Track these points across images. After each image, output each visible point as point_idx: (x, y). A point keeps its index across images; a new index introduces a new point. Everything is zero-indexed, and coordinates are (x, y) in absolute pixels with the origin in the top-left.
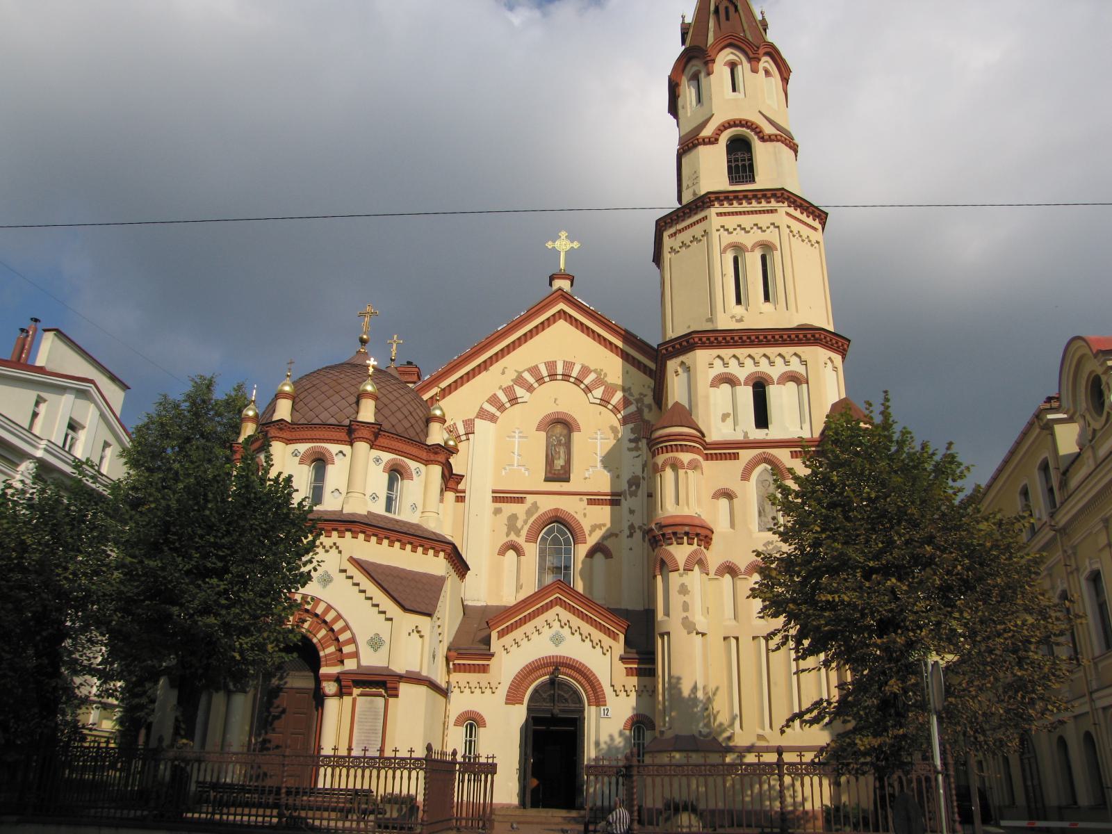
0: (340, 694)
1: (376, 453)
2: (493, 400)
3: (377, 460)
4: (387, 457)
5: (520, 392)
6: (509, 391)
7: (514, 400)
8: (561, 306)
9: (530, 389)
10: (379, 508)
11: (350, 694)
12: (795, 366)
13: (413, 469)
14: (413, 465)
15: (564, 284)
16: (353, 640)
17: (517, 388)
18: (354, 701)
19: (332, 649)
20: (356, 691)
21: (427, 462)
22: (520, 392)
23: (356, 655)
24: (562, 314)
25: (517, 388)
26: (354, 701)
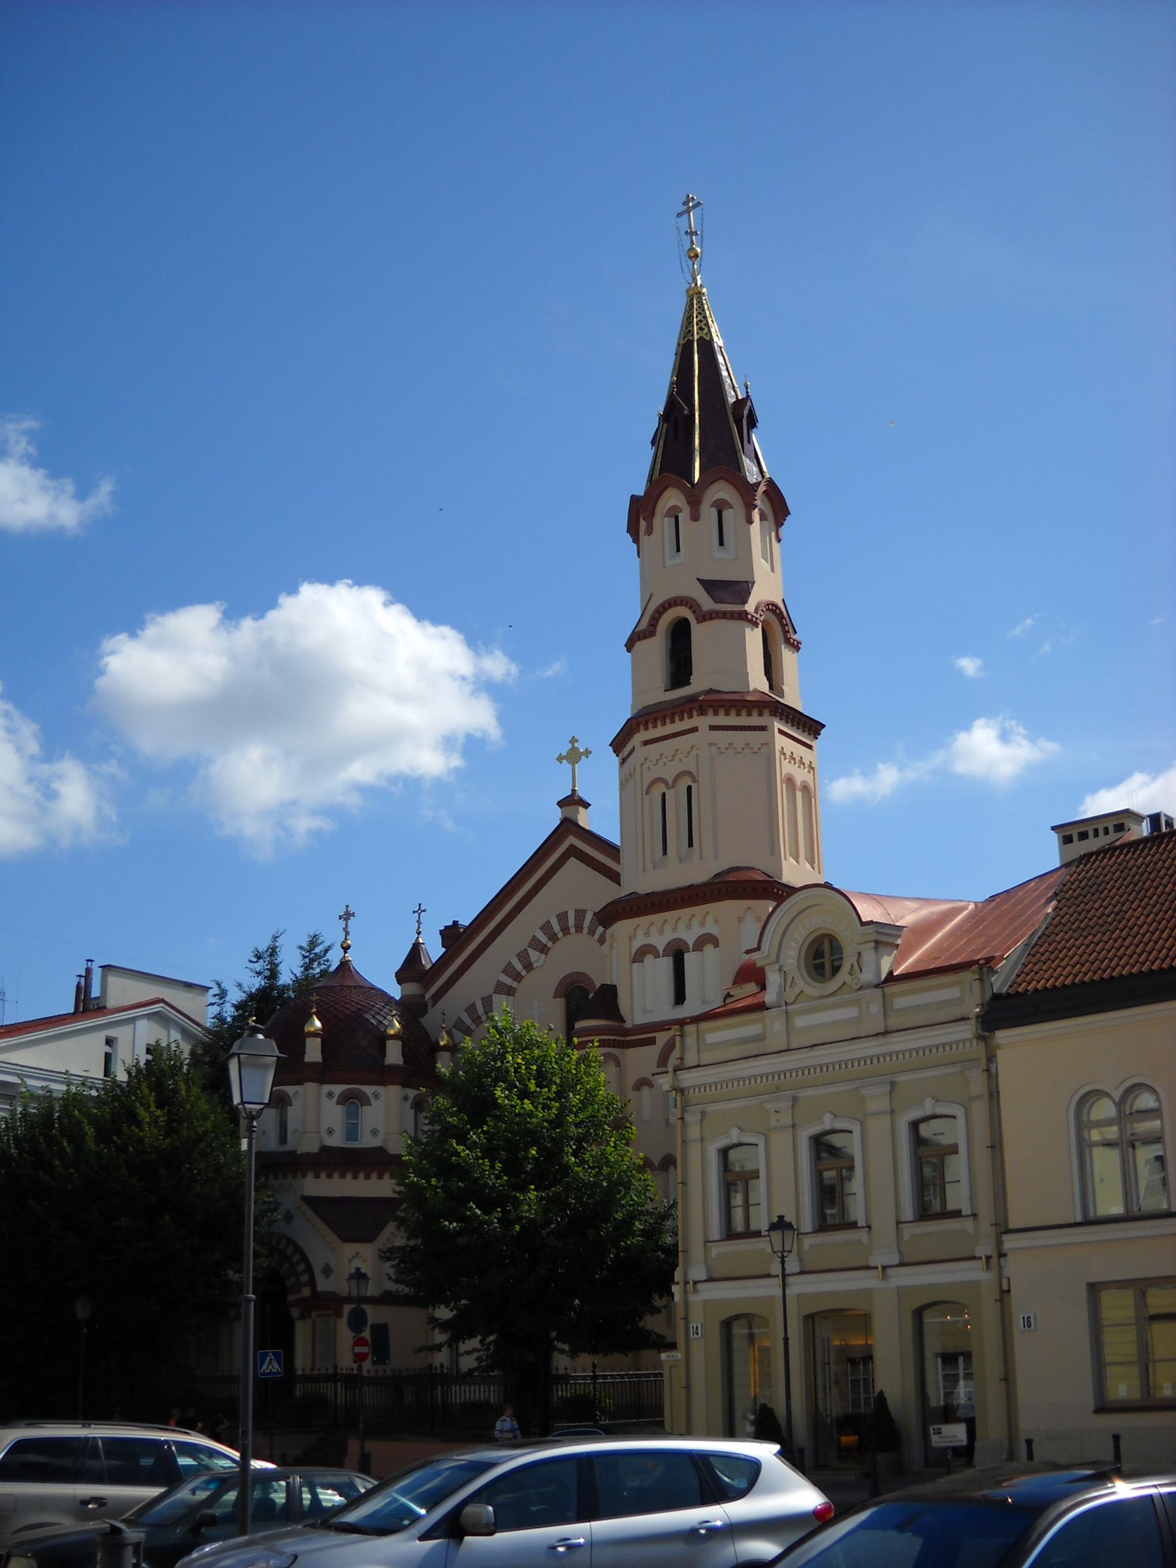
0: (303, 1317)
1: (327, 1088)
2: (509, 970)
3: (330, 1095)
4: (338, 1089)
5: (534, 955)
6: (523, 956)
7: (529, 966)
8: (572, 840)
9: (544, 950)
10: (337, 1141)
11: (310, 1316)
12: (711, 928)
13: (369, 1095)
14: (369, 1090)
15: (569, 810)
16: (309, 1270)
17: (530, 950)
18: (314, 1321)
19: (293, 1280)
20: (314, 1314)
21: (383, 1083)
22: (534, 955)
23: (312, 1283)
24: (573, 852)
25: (530, 950)
26: (314, 1321)
